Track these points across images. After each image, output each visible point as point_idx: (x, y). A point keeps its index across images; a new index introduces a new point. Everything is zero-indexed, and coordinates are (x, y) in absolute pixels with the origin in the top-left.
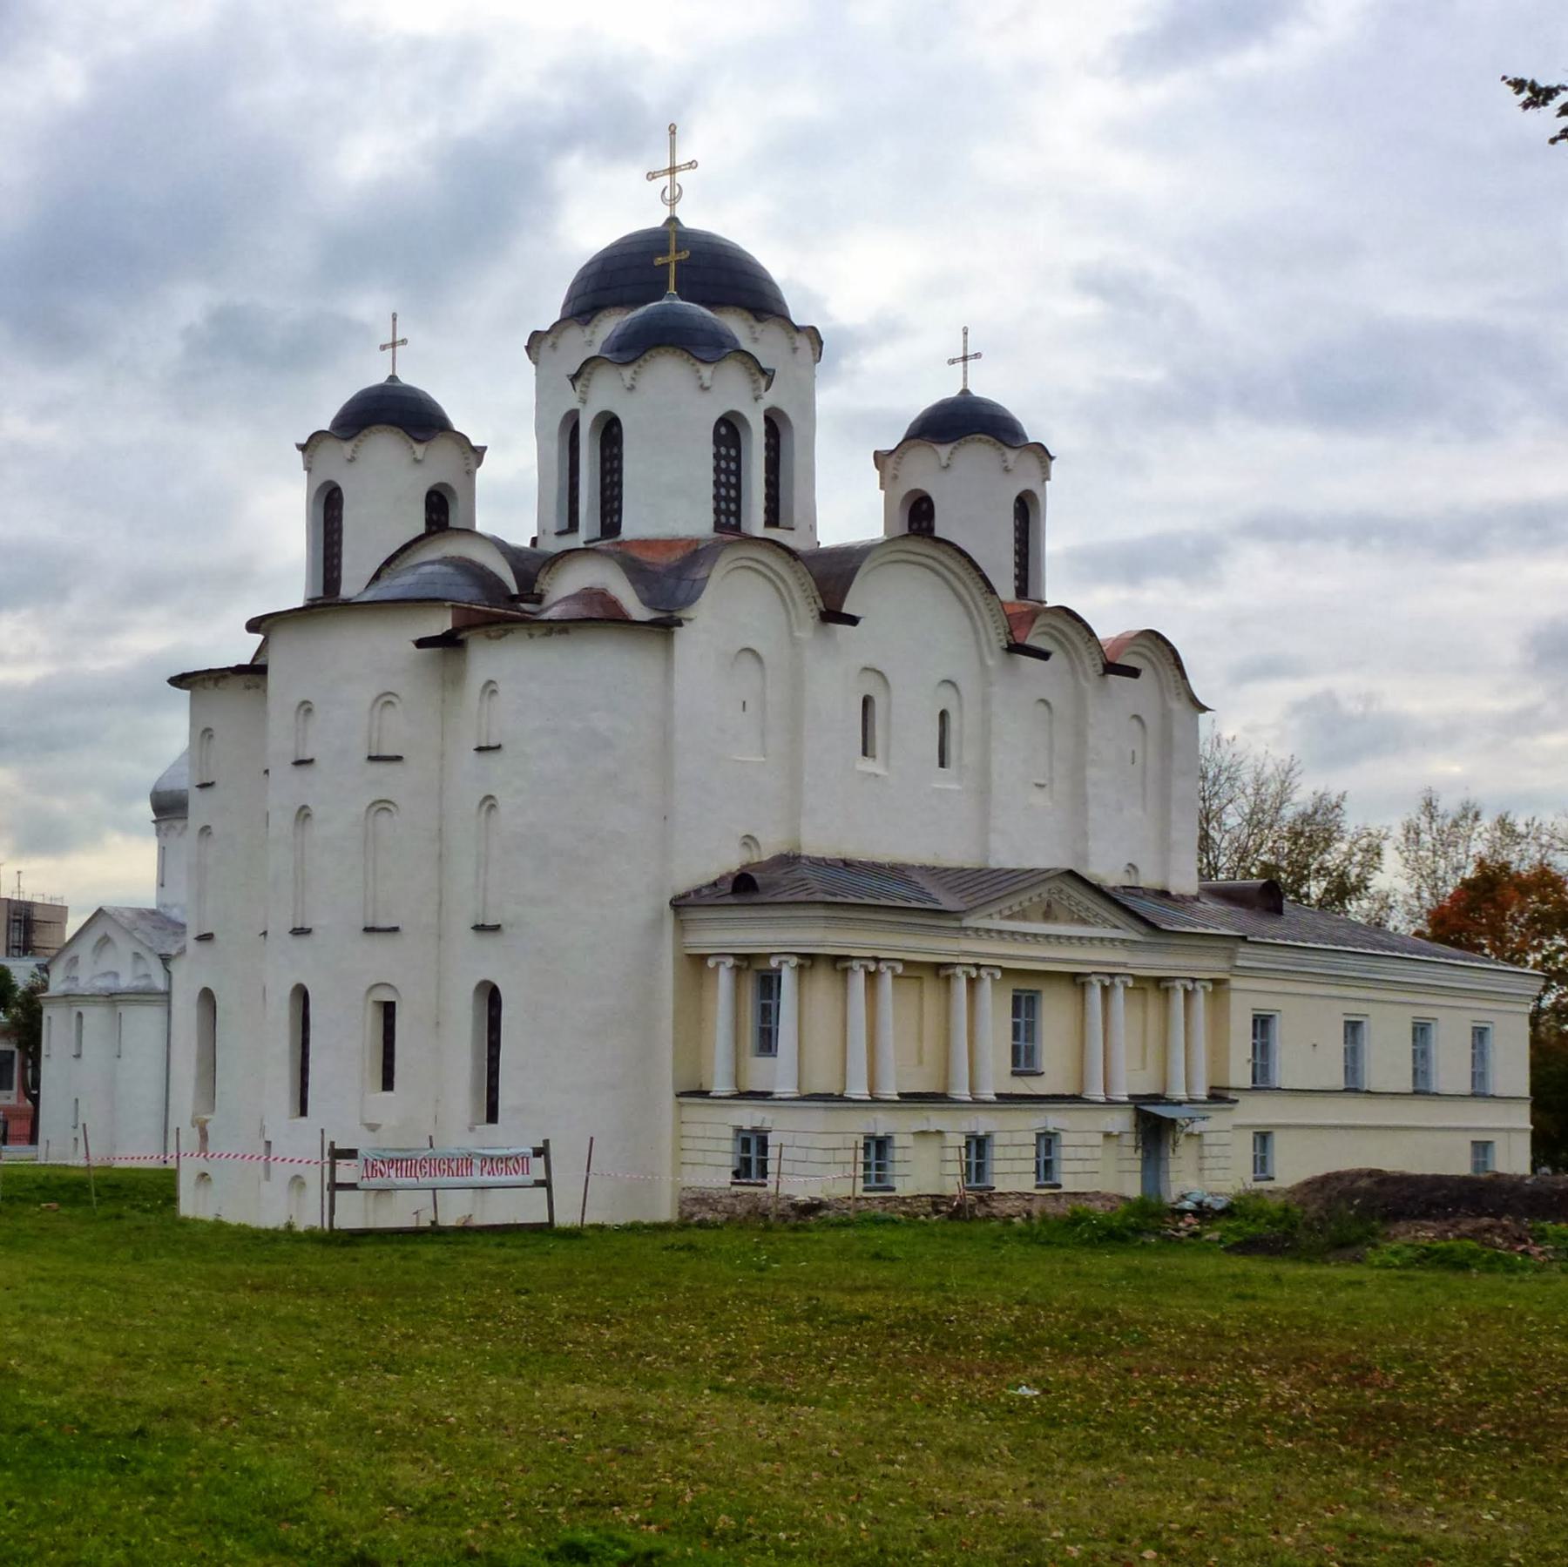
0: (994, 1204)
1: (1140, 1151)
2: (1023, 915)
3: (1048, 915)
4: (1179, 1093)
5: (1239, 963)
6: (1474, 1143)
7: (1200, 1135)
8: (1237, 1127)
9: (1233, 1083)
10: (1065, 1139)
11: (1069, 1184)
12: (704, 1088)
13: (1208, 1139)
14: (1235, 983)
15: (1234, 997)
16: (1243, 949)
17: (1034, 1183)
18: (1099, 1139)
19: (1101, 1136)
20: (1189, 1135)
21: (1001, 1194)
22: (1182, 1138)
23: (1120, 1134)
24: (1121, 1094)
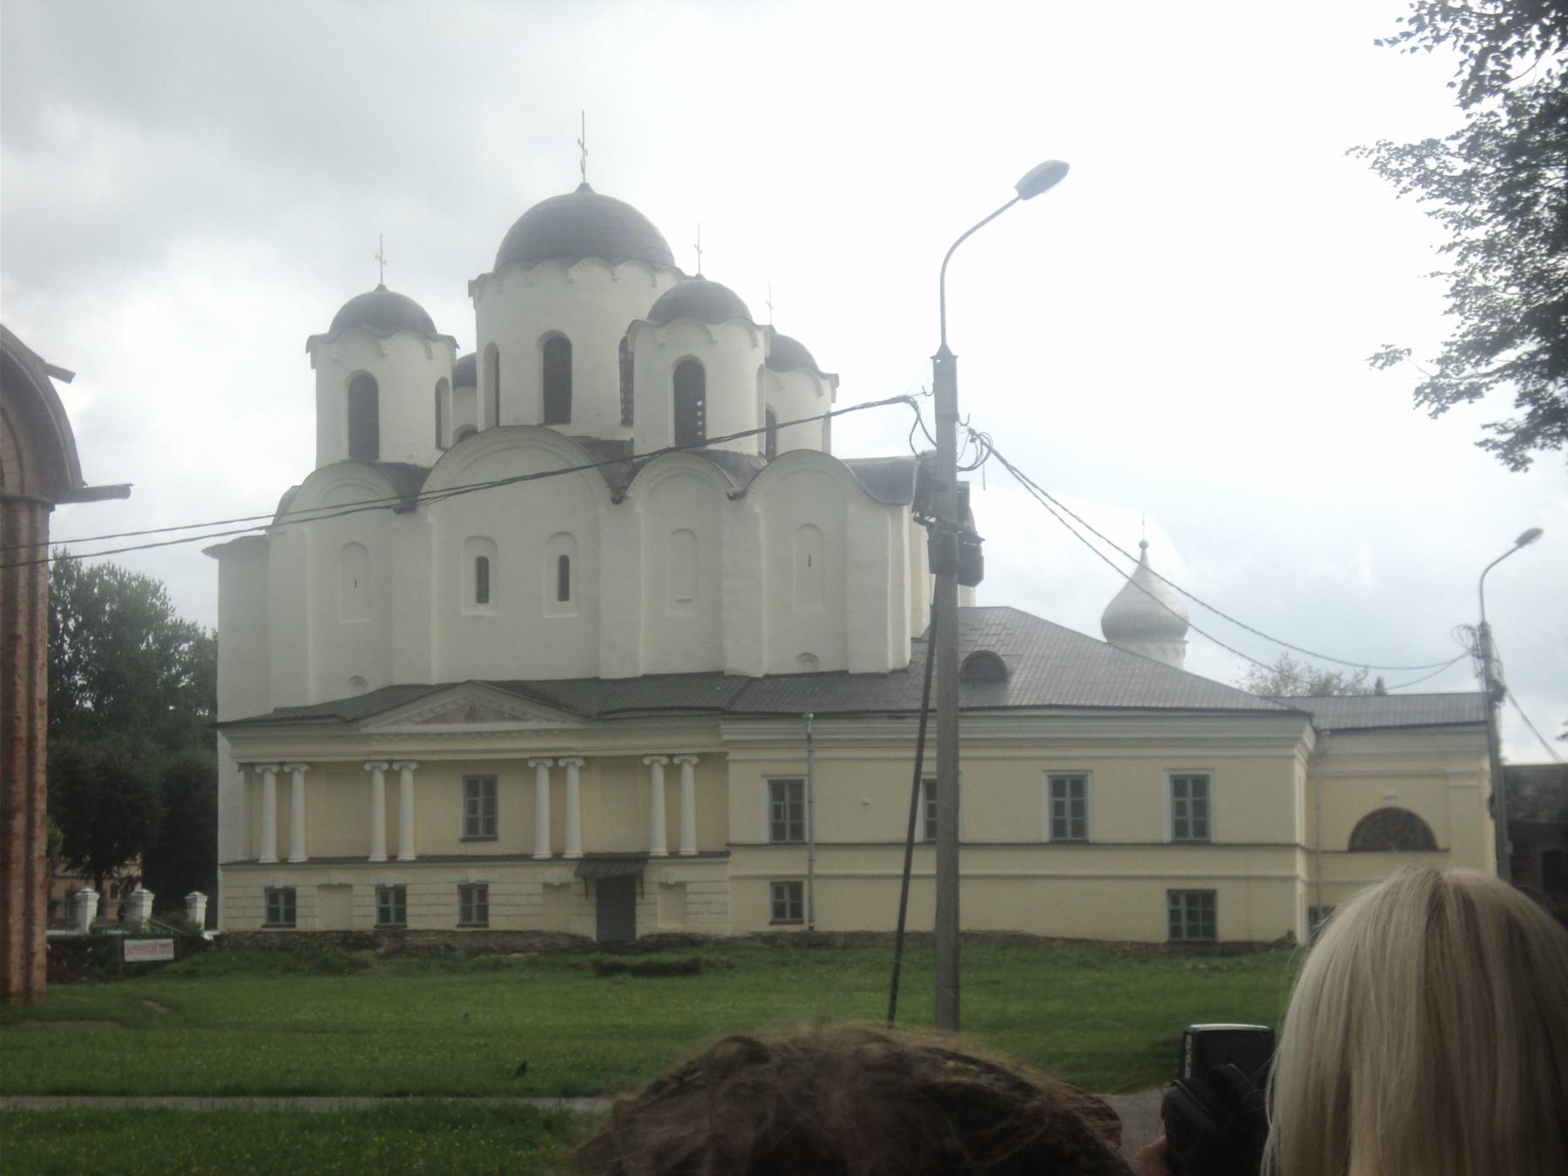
0: (408, 938)
1: (593, 900)
2: (442, 719)
3: (472, 716)
4: (660, 849)
5: (725, 737)
6: (1169, 892)
7: (681, 886)
8: (734, 878)
9: (734, 839)
10: (492, 889)
11: (497, 922)
12: (254, 857)
13: (689, 888)
14: (733, 755)
15: (734, 769)
16: (724, 726)
17: (458, 923)
18: (539, 889)
19: (541, 886)
20: (664, 886)
21: (415, 931)
22: (647, 888)
23: (564, 886)
24: (575, 850)
